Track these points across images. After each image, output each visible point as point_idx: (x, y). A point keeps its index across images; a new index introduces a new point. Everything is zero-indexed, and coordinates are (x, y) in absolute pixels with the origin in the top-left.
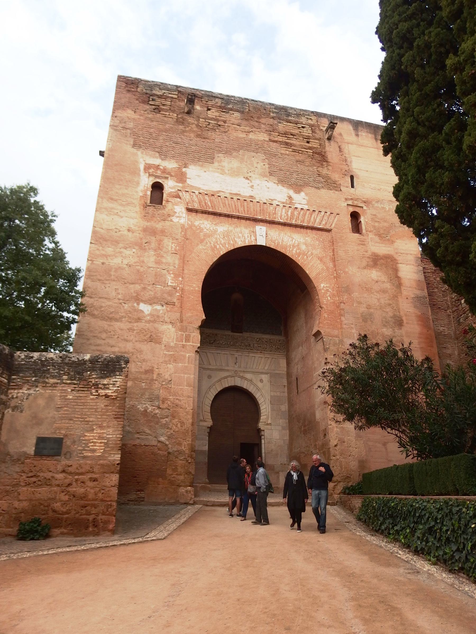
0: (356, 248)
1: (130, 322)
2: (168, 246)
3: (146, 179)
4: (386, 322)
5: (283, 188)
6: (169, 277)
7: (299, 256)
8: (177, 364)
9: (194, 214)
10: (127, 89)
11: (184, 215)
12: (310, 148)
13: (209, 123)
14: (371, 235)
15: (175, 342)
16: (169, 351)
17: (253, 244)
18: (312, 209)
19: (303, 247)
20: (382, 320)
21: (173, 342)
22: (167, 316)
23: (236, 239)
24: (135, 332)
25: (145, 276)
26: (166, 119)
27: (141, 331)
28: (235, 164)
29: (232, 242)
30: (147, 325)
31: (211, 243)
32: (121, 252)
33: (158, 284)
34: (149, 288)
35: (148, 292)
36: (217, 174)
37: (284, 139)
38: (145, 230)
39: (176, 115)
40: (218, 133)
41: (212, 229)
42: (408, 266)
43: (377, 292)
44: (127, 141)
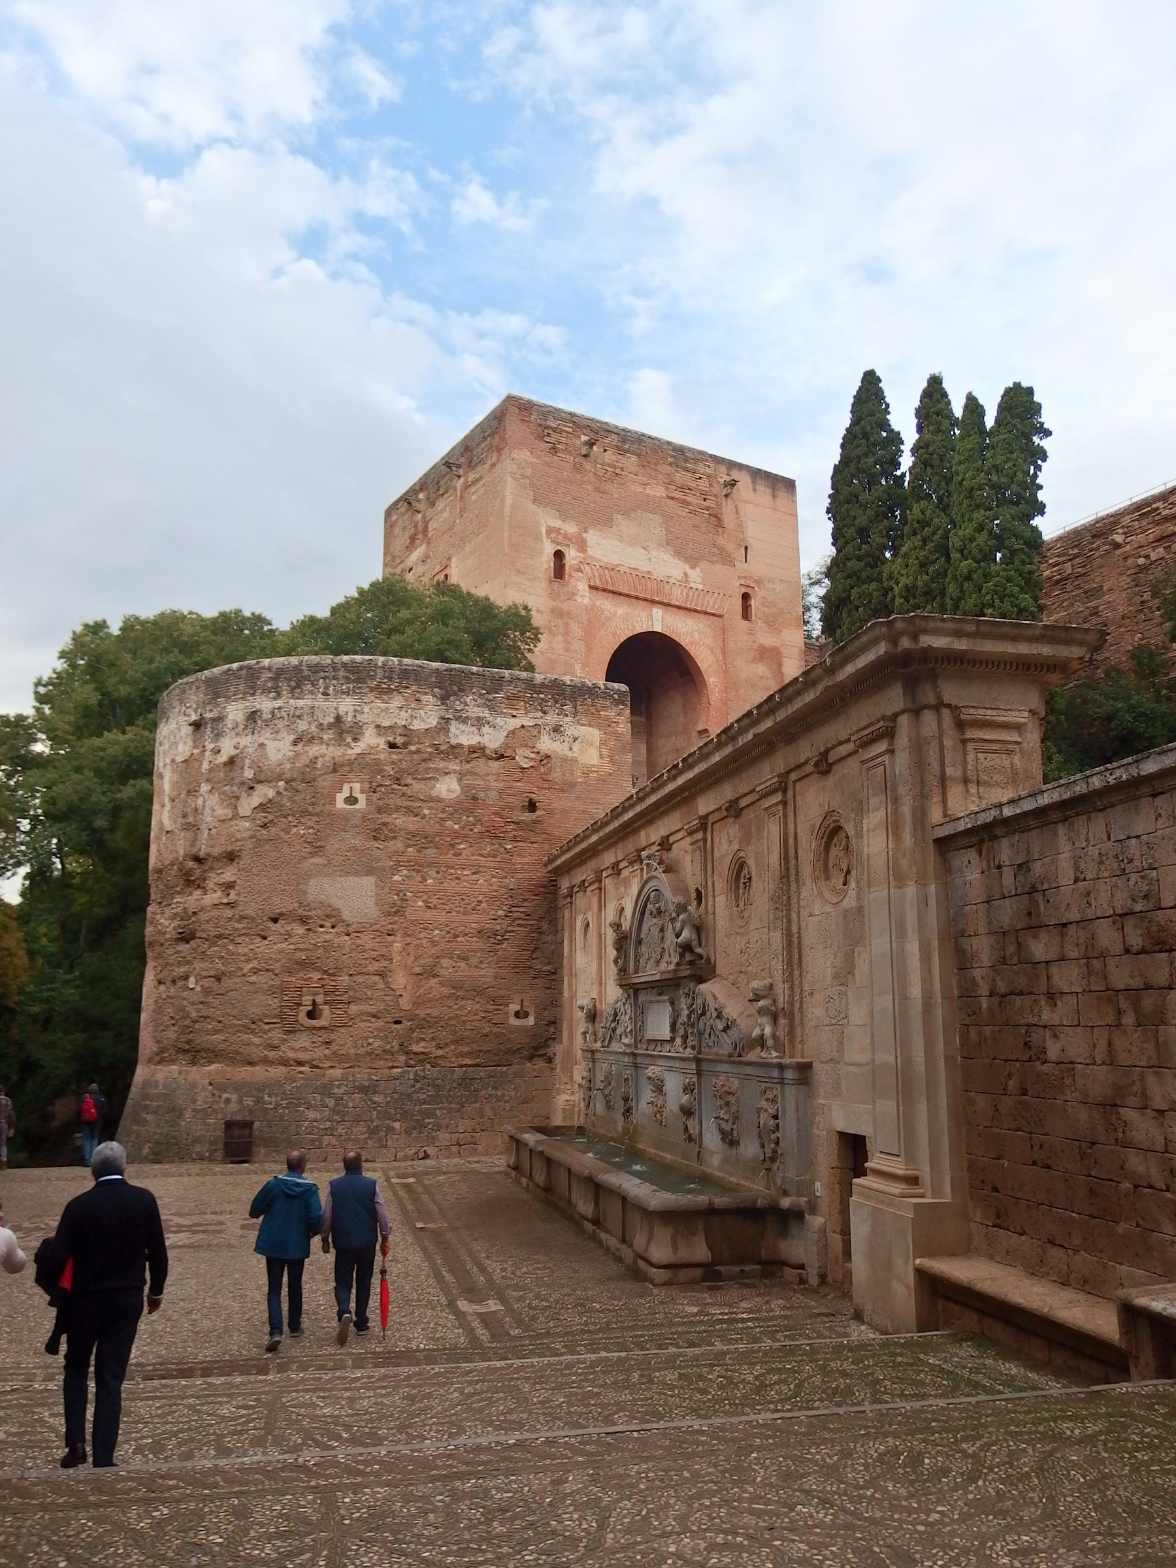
14: (760, 623)
36: (616, 542)
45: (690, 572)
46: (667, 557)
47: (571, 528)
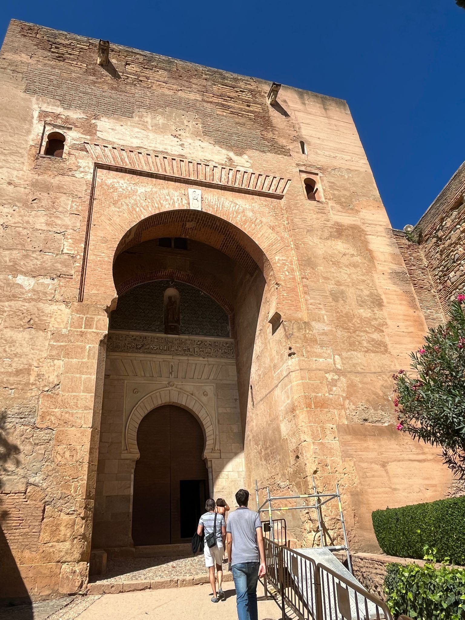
0: (314, 216)
2: (66, 204)
4: (362, 302)
5: (221, 149)
6: (65, 243)
7: (245, 224)
8: (70, 360)
12: (251, 112)
13: (128, 77)
14: (331, 203)
15: (69, 328)
16: (58, 341)
17: (185, 208)
18: (257, 173)
19: (250, 214)
20: (357, 299)
21: (67, 328)
22: (59, 292)
23: (162, 202)
24: (5, 314)
25: (29, 240)
27: (15, 312)
28: (161, 120)
29: (157, 206)
30: (26, 304)
31: (128, 205)
33: (48, 251)
34: (34, 255)
35: (31, 260)
36: (137, 130)
37: (220, 101)
38: (35, 185)
39: (85, 65)
41: (129, 189)
42: (379, 238)
43: (347, 266)
46: (205, 144)
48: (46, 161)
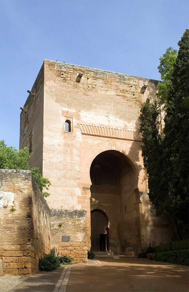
1: (63, 187)
3: (63, 119)
5: (122, 121)
9: (84, 136)
10: (49, 68)
11: (81, 137)
12: (135, 98)
17: (110, 149)
24: (65, 191)
26: (69, 85)
32: (56, 156)
38: (65, 144)
40: (93, 92)
44: (53, 98)
45: (128, 125)
46: (117, 119)
47: (72, 111)
48: (66, 134)
